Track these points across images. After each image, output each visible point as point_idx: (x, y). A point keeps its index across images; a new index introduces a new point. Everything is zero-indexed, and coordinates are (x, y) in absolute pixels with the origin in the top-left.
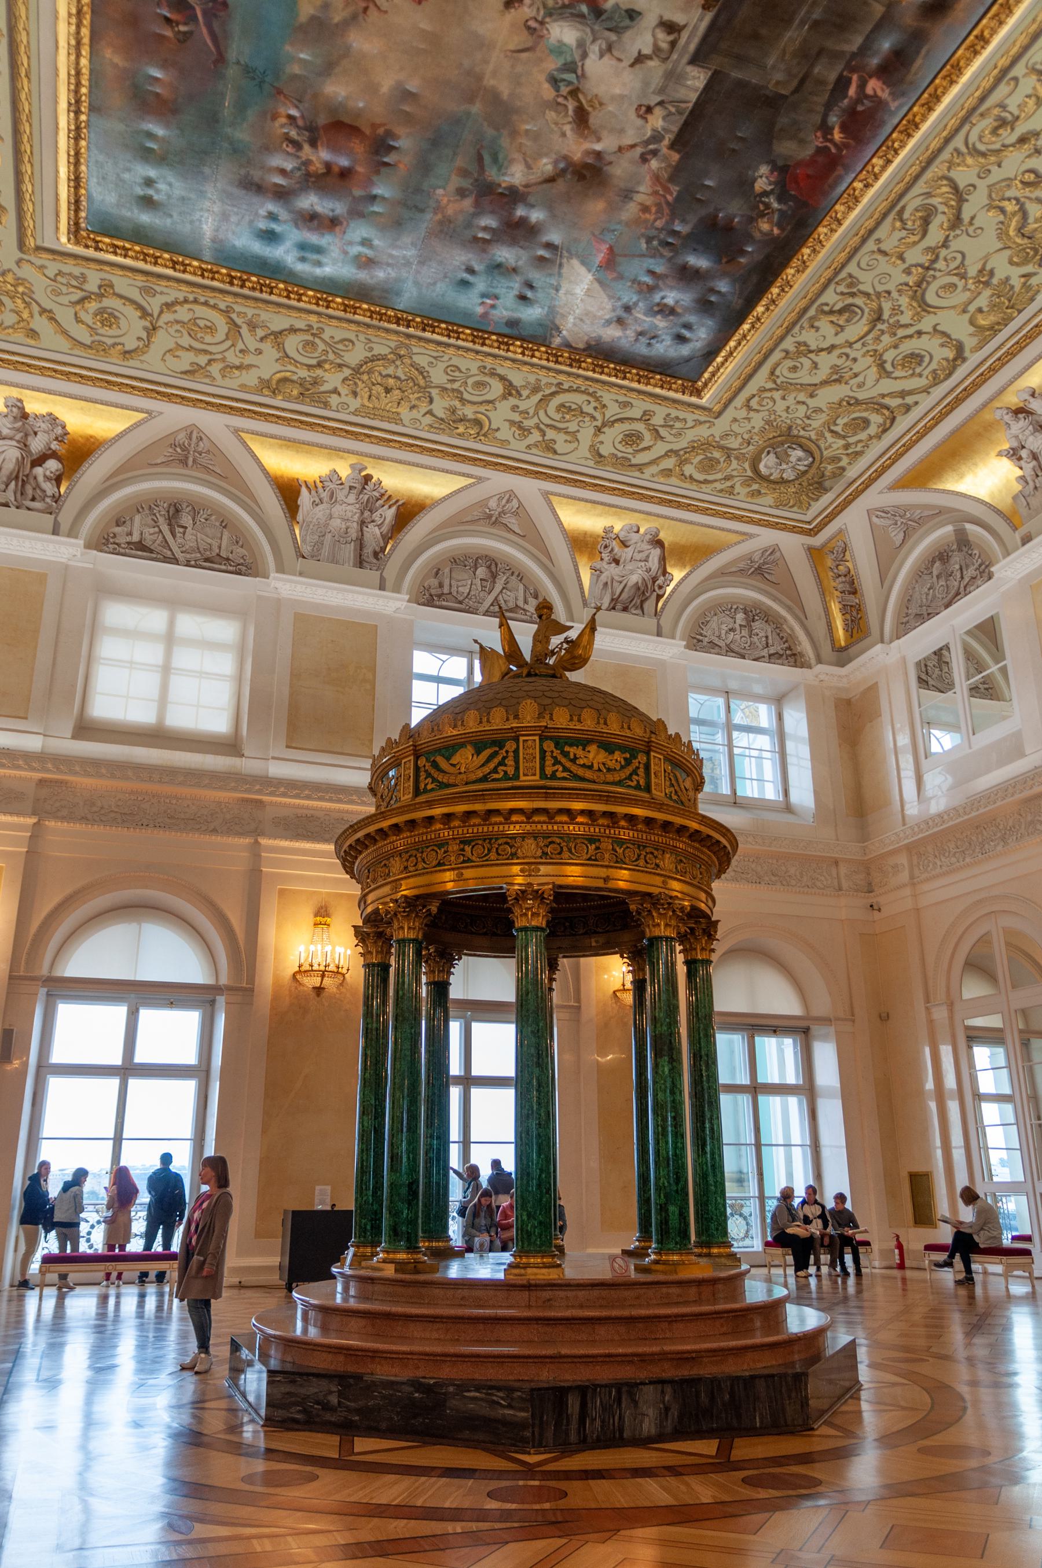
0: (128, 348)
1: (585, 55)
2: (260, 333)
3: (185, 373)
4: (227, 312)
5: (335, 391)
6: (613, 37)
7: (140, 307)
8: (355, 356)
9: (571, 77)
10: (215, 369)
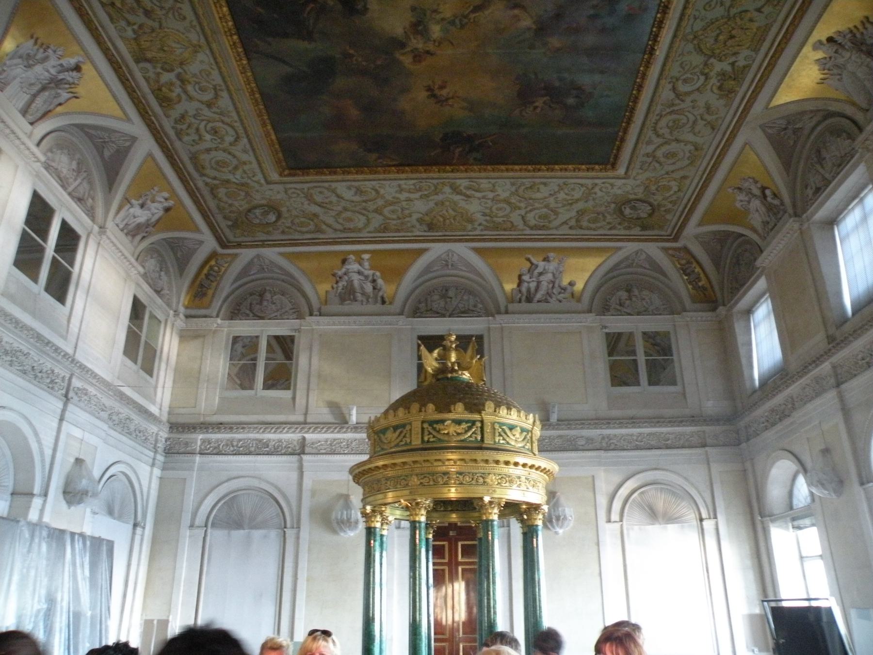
0: (692, 148)
1: (443, 19)
2: (677, 101)
3: (713, 129)
4: (661, 116)
5: (733, 64)
6: (428, 13)
7: (662, 145)
8: (697, 60)
9: (457, 21)
10: (707, 117)
